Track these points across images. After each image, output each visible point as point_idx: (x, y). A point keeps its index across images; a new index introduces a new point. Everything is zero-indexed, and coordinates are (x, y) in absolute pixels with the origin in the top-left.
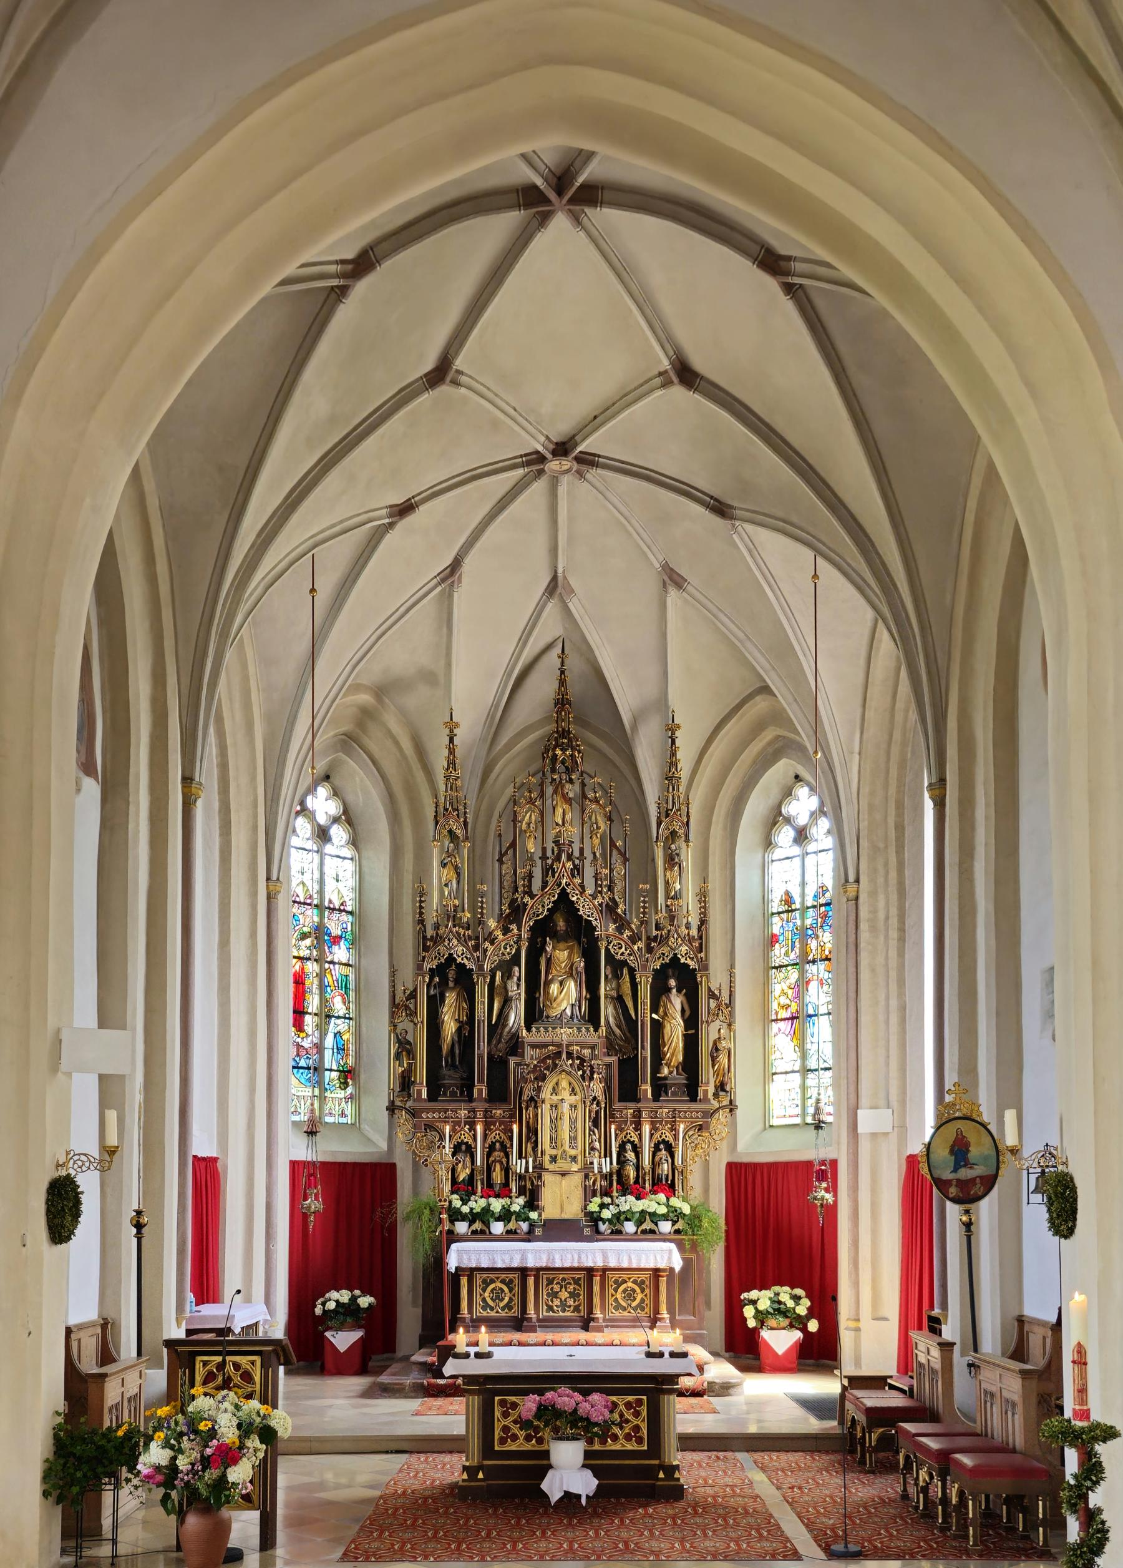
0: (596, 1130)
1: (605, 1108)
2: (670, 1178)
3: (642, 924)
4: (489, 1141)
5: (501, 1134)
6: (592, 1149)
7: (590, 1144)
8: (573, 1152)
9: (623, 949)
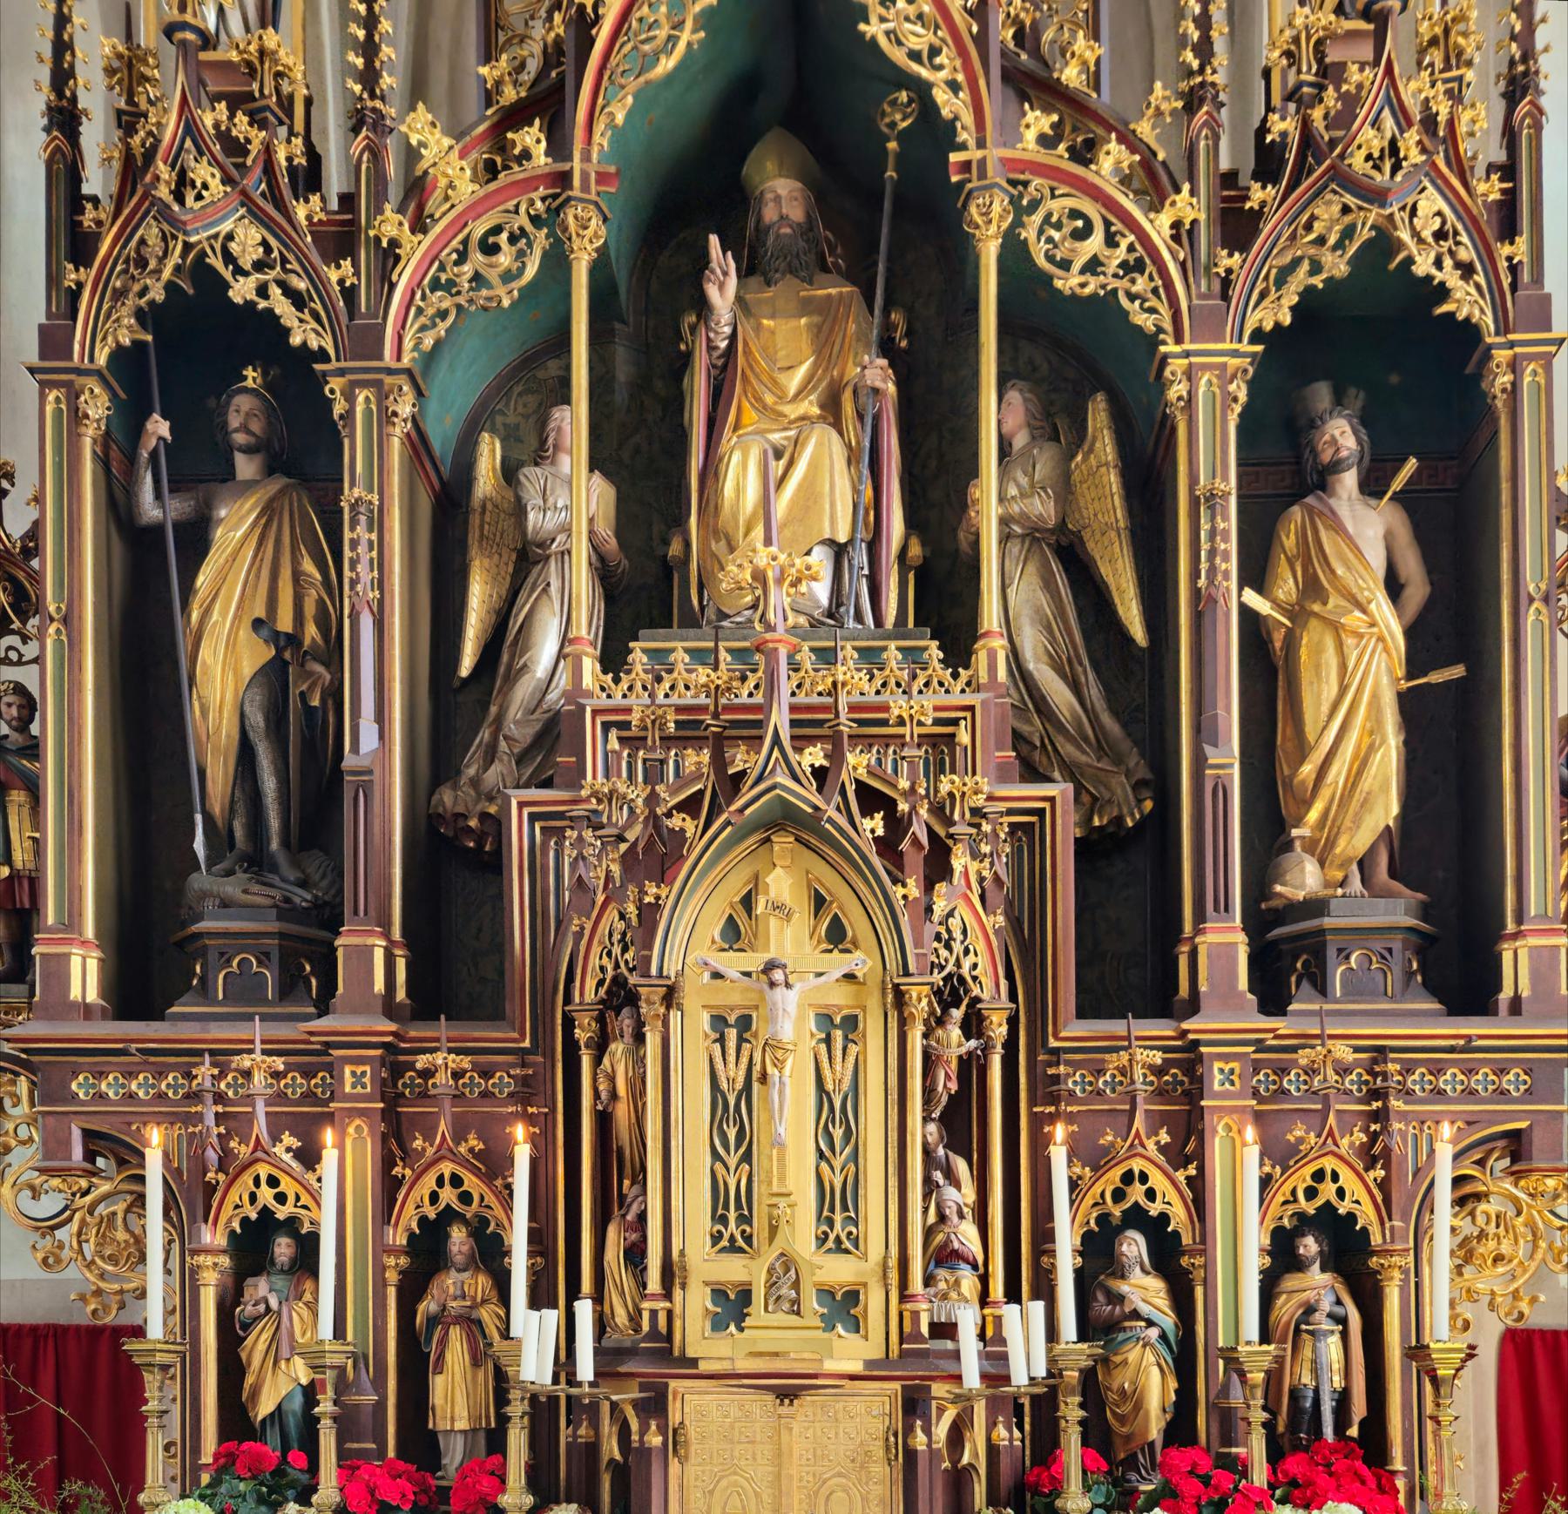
0: (961, 1166)
1: (1011, 1045)
2: (1359, 1409)
3: (1190, 108)
4: (408, 1219)
5: (471, 1182)
6: (945, 1257)
7: (929, 1233)
8: (840, 1271)
9: (1095, 243)
